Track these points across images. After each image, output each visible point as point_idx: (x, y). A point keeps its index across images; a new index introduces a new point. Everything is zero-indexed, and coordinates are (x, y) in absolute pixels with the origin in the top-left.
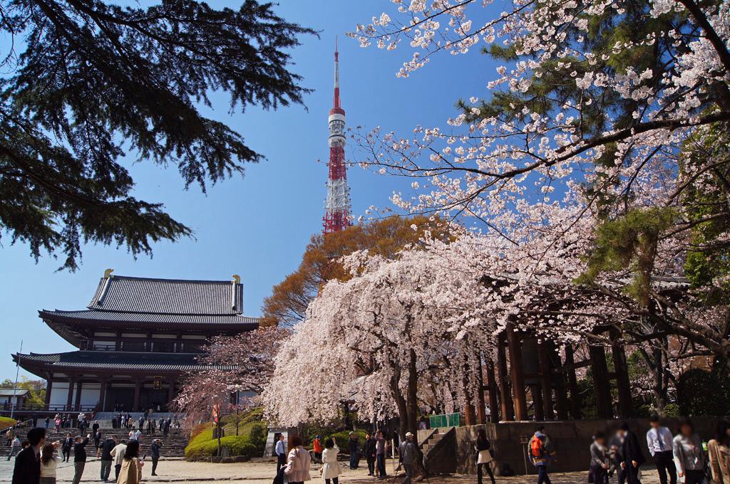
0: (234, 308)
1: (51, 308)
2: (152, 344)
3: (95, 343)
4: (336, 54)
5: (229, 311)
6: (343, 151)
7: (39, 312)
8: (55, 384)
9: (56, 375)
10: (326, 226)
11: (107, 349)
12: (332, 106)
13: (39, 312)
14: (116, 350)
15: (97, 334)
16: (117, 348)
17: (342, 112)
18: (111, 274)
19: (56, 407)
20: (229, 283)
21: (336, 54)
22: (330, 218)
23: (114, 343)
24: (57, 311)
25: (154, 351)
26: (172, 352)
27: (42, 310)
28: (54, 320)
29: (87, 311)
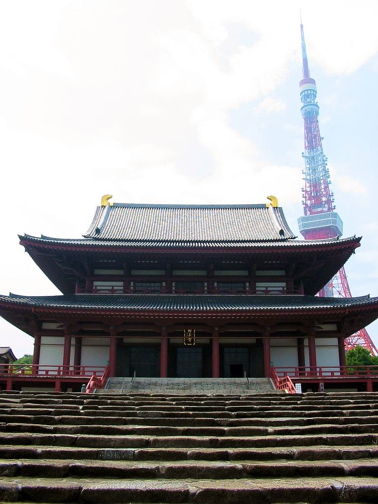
0: (282, 232)
1: (36, 233)
2: (174, 284)
3: (96, 283)
4: (302, 26)
5: (279, 237)
7: (20, 237)
8: (45, 340)
9: (47, 326)
10: (305, 197)
11: (113, 291)
12: (301, 77)
13: (20, 237)
14: (125, 292)
15: (98, 272)
16: (126, 289)
18: (110, 201)
19: (47, 368)
20: (263, 207)
21: (302, 26)
22: (308, 189)
23: (121, 284)
24: (43, 237)
25: (176, 293)
26: (203, 293)
27: (23, 235)
28: (44, 252)
29: (84, 240)
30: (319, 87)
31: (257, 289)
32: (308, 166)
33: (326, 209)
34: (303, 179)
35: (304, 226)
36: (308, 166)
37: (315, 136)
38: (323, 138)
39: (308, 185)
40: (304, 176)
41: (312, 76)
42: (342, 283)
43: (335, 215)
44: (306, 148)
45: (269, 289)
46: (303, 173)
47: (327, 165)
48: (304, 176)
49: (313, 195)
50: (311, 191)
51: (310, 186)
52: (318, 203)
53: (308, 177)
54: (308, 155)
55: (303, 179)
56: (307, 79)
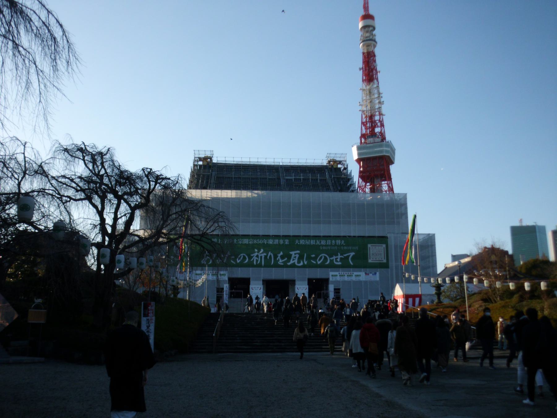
6: (375, 56)
12: (362, 13)
17: (371, 17)
22: (364, 120)
30: (378, 23)
32: (364, 98)
33: (379, 140)
35: (359, 154)
36: (364, 98)
37: (372, 71)
39: (364, 116)
40: (360, 108)
41: (371, 12)
43: (389, 145)
44: (363, 81)
48: (360, 108)
50: (366, 122)
51: (366, 117)
52: (373, 134)
53: (365, 109)
54: (364, 88)
56: (367, 16)
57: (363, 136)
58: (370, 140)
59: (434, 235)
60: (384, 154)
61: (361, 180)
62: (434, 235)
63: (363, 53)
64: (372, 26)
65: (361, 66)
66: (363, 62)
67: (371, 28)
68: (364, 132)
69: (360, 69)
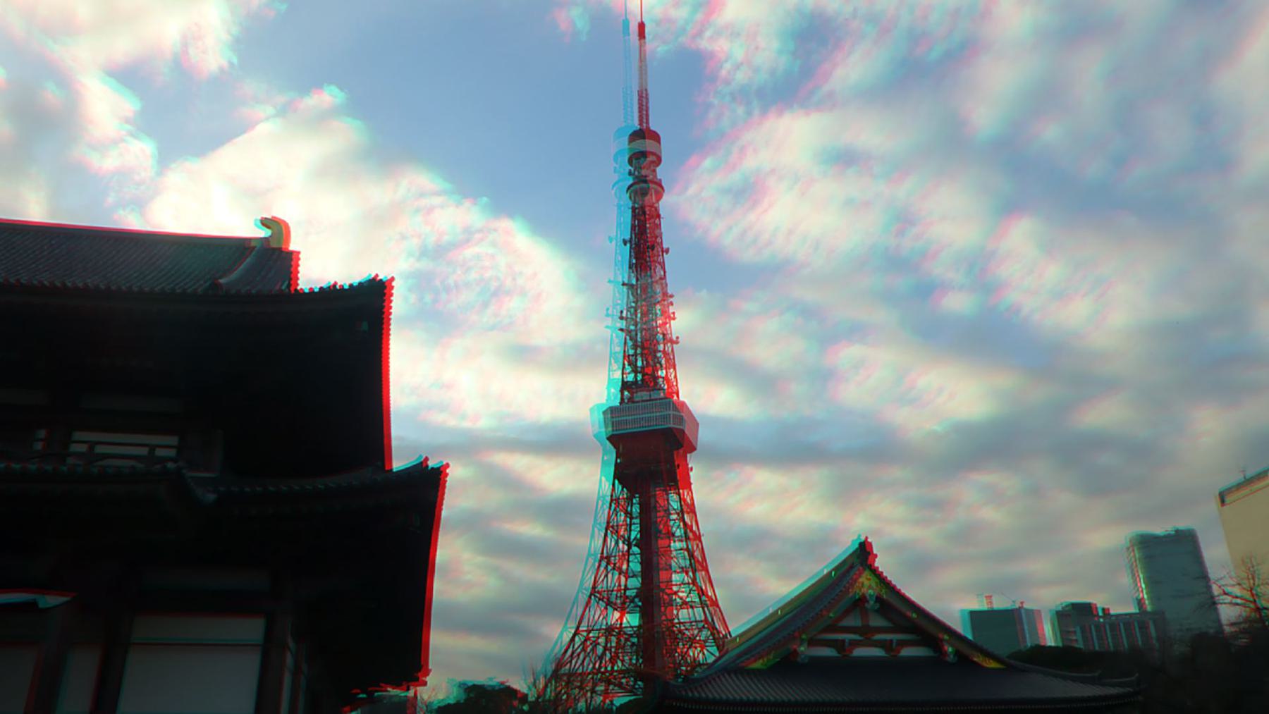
6: (659, 216)
17: (656, 137)
31: (75, 448)
34: (621, 330)
37: (652, 248)
38: (667, 251)
40: (623, 324)
42: (687, 549)
45: (99, 449)
46: (621, 318)
47: (672, 304)
48: (623, 324)
49: (639, 364)
50: (635, 355)
51: (635, 346)
53: (632, 328)
55: (621, 330)
56: (643, 133)
57: (625, 386)
58: (642, 395)
59: (299, 253)
60: (672, 426)
61: (618, 487)
62: (299, 253)
63: (634, 209)
64: (654, 154)
65: (628, 237)
66: (633, 227)
67: (652, 158)
68: (630, 378)
69: (625, 242)
